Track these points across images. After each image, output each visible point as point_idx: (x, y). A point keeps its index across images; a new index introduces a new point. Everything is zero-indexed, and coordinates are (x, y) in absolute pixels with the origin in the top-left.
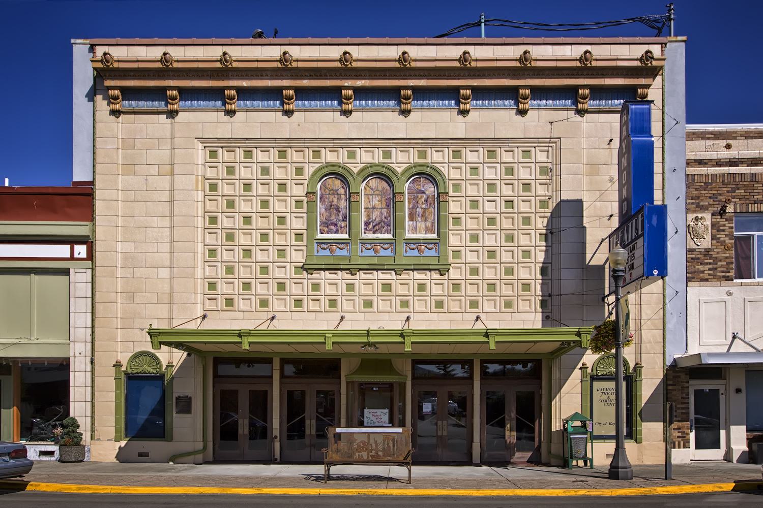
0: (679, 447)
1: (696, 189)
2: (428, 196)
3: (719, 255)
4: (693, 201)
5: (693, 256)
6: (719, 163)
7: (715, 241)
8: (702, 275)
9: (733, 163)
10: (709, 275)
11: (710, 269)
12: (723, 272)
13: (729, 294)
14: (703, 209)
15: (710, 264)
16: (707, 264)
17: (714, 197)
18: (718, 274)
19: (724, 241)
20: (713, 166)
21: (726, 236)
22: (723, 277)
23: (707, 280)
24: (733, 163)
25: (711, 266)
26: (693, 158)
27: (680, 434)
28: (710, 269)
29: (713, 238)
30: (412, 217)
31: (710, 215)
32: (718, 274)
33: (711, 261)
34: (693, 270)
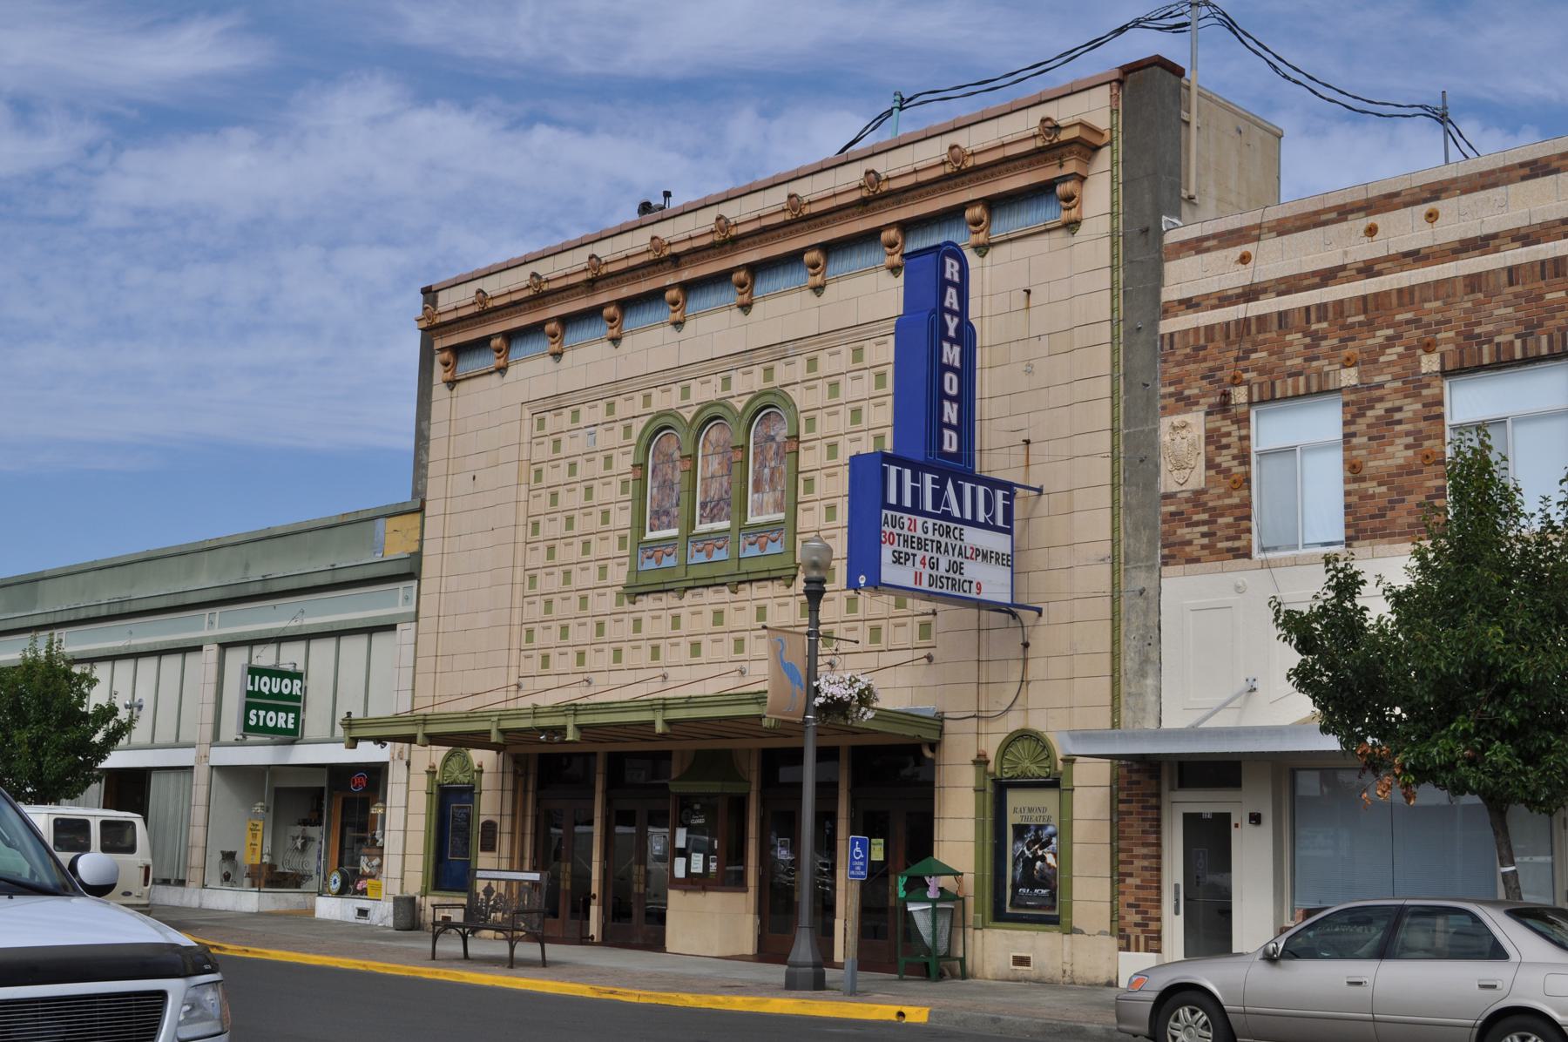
0: (1137, 950)
1: (1178, 364)
2: (779, 444)
3: (1220, 503)
4: (1172, 389)
5: (1172, 508)
6: (1224, 300)
7: (1212, 472)
8: (1188, 549)
9: (1251, 293)
10: (1203, 547)
11: (1204, 535)
12: (1228, 539)
13: (1238, 589)
14: (1188, 403)
15: (1204, 523)
16: (1197, 524)
17: (1208, 376)
18: (1220, 545)
19: (1229, 470)
20: (1214, 307)
21: (1234, 458)
22: (1229, 550)
23: (1197, 560)
24: (1251, 293)
25: (1205, 529)
26: (1176, 297)
27: (1138, 918)
28: (1204, 535)
29: (1210, 464)
30: (757, 489)
31: (1202, 414)
32: (1220, 545)
33: (1205, 516)
34: (1172, 539)
